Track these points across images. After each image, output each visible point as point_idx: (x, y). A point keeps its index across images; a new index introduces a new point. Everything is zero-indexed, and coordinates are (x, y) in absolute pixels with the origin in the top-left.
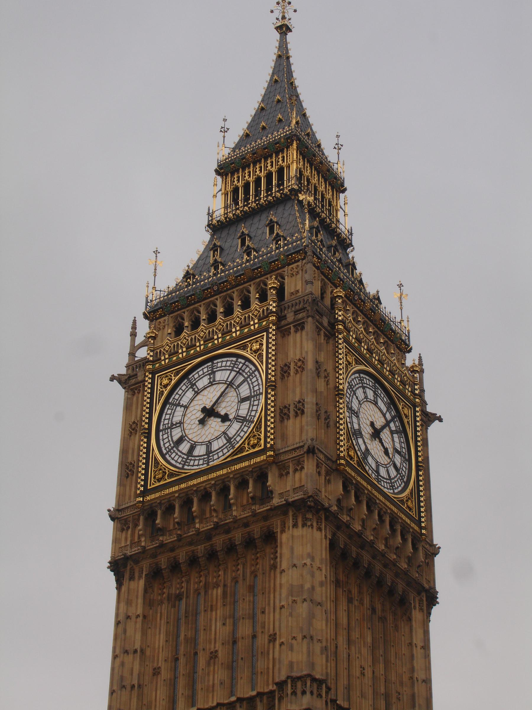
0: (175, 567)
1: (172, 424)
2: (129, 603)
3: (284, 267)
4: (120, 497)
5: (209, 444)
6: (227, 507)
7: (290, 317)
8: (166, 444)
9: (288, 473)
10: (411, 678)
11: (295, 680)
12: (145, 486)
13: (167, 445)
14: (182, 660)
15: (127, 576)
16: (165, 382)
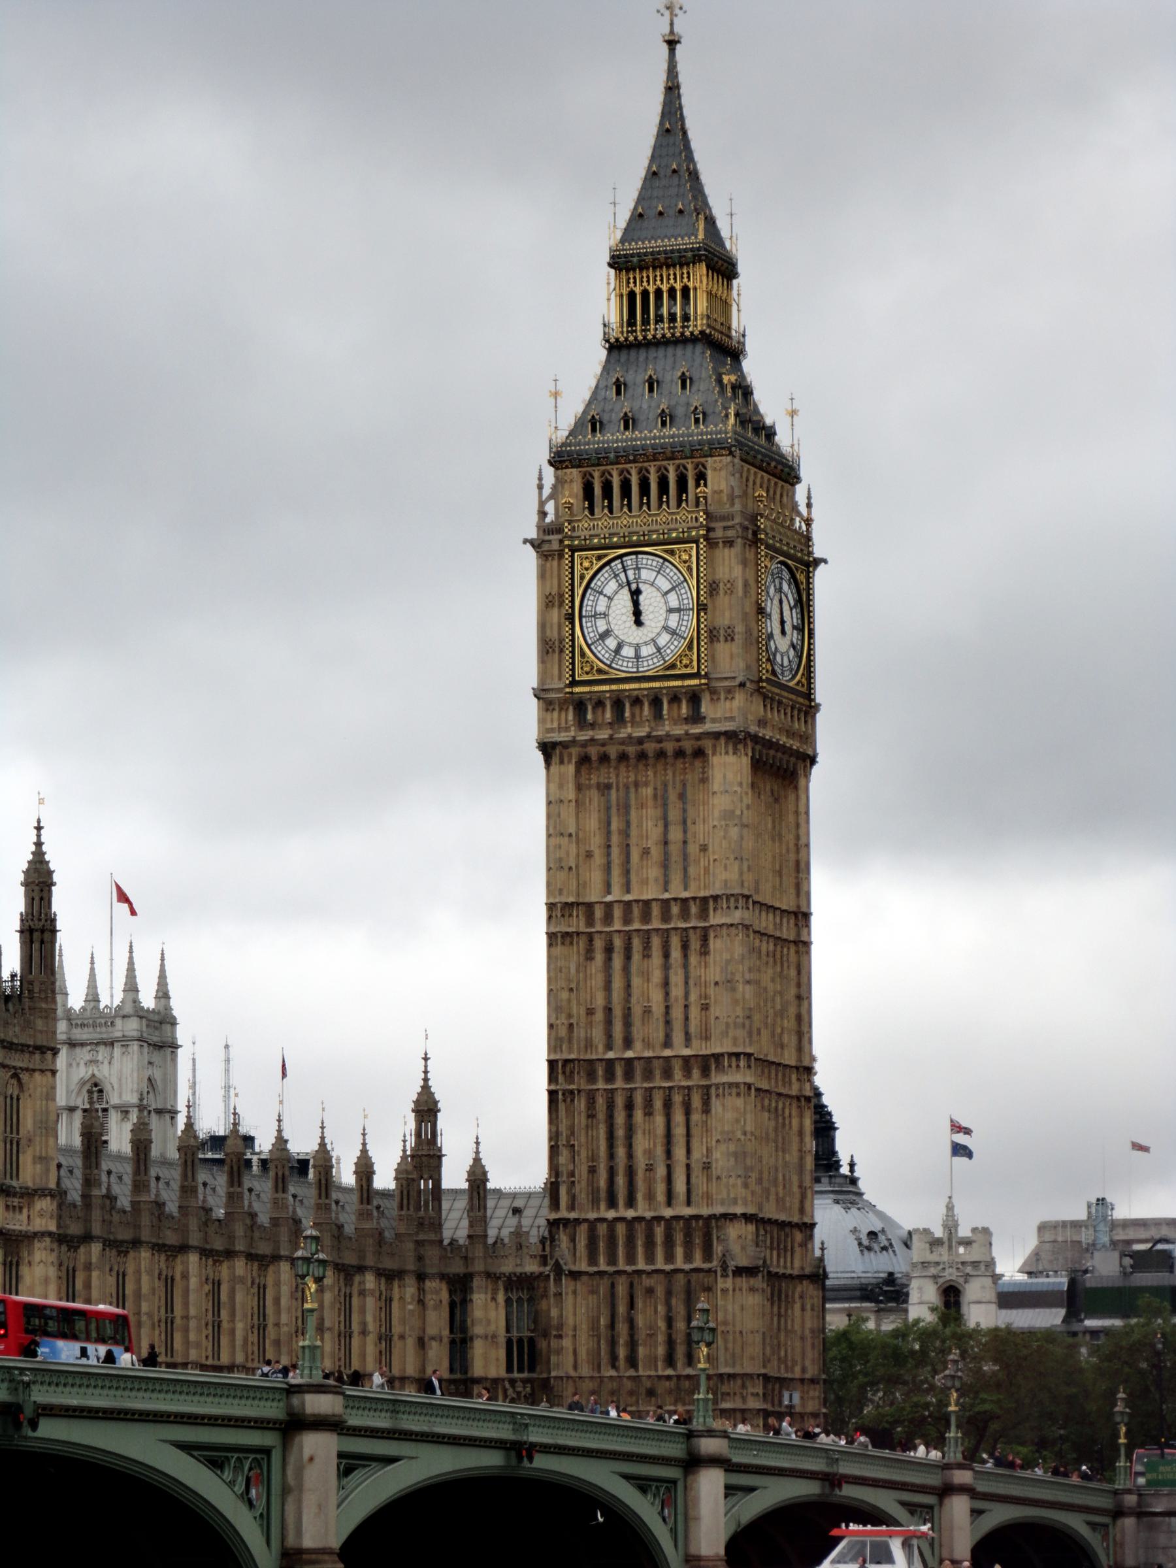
0: (604, 758)
1: (596, 613)
2: (561, 786)
3: (706, 456)
4: (543, 675)
5: (637, 648)
6: (658, 715)
7: (719, 533)
8: (591, 636)
9: (719, 699)
10: (796, 845)
11: (728, 897)
12: (573, 676)
13: (592, 635)
14: (615, 851)
15: (555, 759)
16: (586, 564)
